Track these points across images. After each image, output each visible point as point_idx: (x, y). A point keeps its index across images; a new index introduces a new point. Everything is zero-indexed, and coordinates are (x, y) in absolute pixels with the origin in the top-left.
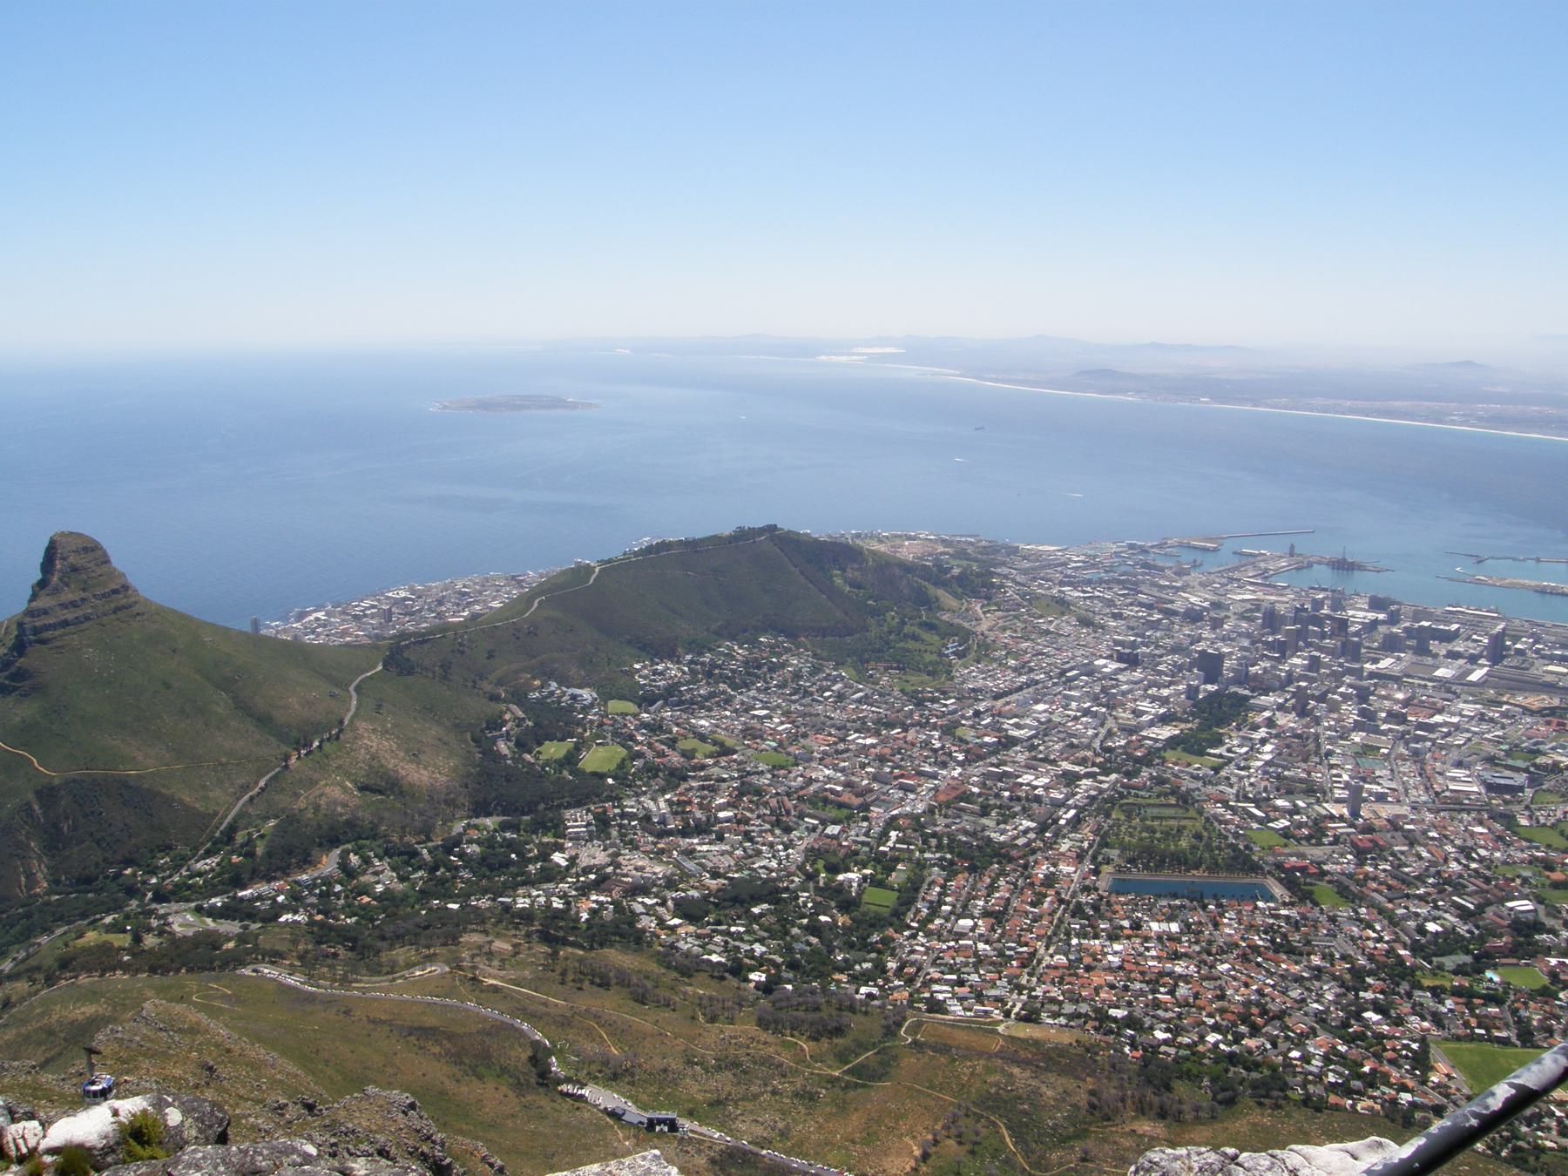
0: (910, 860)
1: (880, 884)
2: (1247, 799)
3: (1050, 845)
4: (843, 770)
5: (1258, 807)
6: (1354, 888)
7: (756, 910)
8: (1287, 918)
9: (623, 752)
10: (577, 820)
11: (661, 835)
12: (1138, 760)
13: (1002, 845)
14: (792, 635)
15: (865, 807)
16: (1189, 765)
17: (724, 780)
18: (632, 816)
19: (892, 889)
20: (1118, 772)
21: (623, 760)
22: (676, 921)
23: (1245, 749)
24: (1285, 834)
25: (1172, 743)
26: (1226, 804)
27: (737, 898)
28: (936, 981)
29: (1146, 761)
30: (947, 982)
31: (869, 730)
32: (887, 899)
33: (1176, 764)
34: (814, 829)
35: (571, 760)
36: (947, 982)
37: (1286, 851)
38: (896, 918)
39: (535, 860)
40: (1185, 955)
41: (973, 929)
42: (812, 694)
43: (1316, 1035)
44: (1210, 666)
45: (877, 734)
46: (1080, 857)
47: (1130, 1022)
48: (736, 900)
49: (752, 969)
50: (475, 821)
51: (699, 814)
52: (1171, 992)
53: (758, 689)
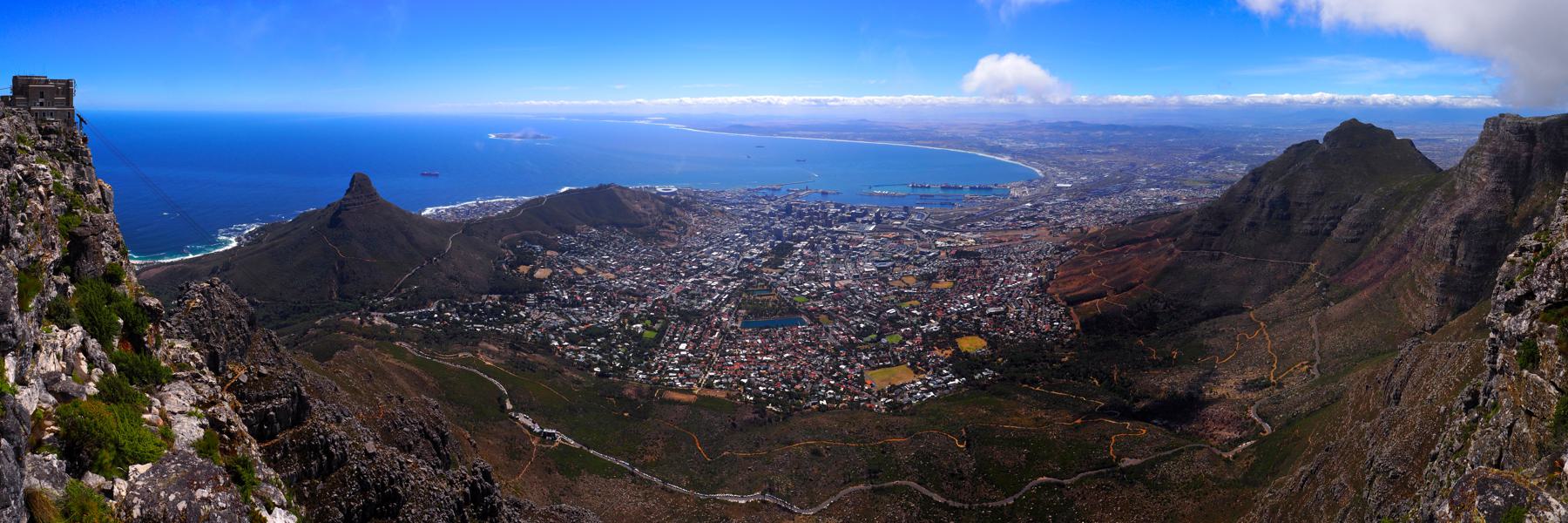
14: (619, 226)
24: (808, 297)
25: (765, 265)
27: (590, 334)
44: (778, 234)
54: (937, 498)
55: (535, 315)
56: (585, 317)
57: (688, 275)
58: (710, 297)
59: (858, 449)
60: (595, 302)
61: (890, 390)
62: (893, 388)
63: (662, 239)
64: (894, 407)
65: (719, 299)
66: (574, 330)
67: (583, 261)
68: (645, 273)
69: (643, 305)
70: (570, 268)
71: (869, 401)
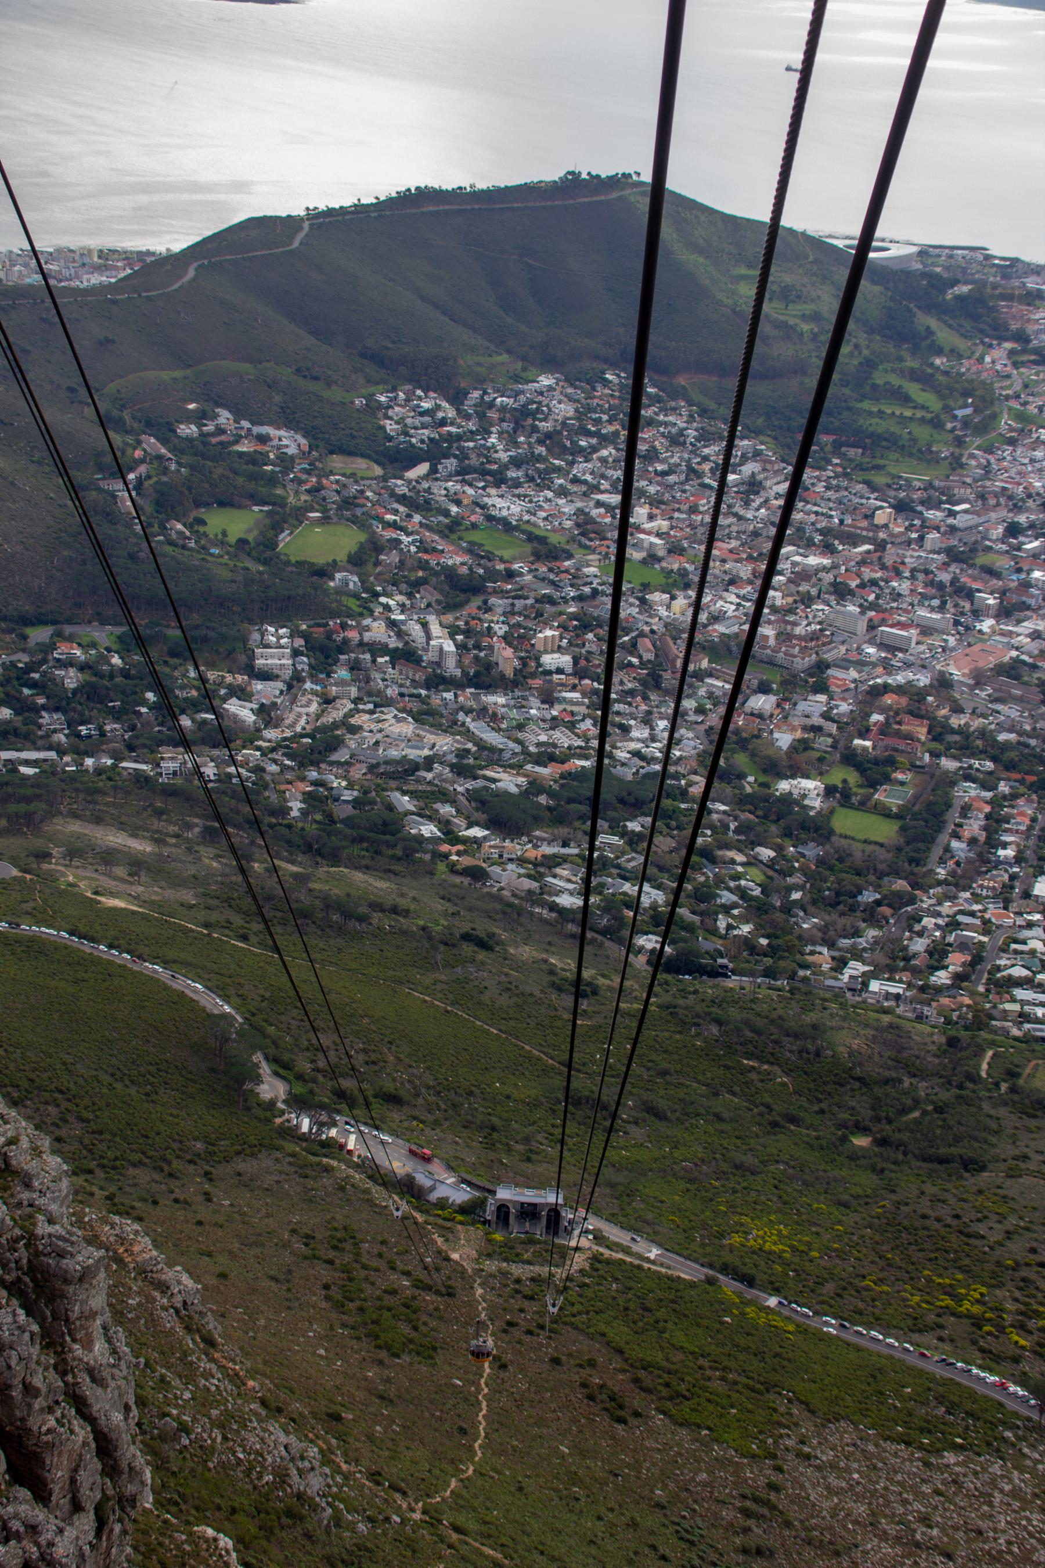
1: (863, 806)
7: (634, 826)
9: (363, 537)
10: (276, 647)
11: (437, 681)
17: (552, 601)
18: (376, 649)
19: (885, 813)
21: (362, 546)
22: (477, 832)
31: (810, 544)
32: (885, 831)
35: (264, 547)
39: (194, 706)
42: (699, 475)
45: (828, 549)
50: (68, 629)
51: (509, 652)
53: (603, 460)
55: (303, 715)
57: (1009, 611)
63: (877, 444)
67: (506, 506)
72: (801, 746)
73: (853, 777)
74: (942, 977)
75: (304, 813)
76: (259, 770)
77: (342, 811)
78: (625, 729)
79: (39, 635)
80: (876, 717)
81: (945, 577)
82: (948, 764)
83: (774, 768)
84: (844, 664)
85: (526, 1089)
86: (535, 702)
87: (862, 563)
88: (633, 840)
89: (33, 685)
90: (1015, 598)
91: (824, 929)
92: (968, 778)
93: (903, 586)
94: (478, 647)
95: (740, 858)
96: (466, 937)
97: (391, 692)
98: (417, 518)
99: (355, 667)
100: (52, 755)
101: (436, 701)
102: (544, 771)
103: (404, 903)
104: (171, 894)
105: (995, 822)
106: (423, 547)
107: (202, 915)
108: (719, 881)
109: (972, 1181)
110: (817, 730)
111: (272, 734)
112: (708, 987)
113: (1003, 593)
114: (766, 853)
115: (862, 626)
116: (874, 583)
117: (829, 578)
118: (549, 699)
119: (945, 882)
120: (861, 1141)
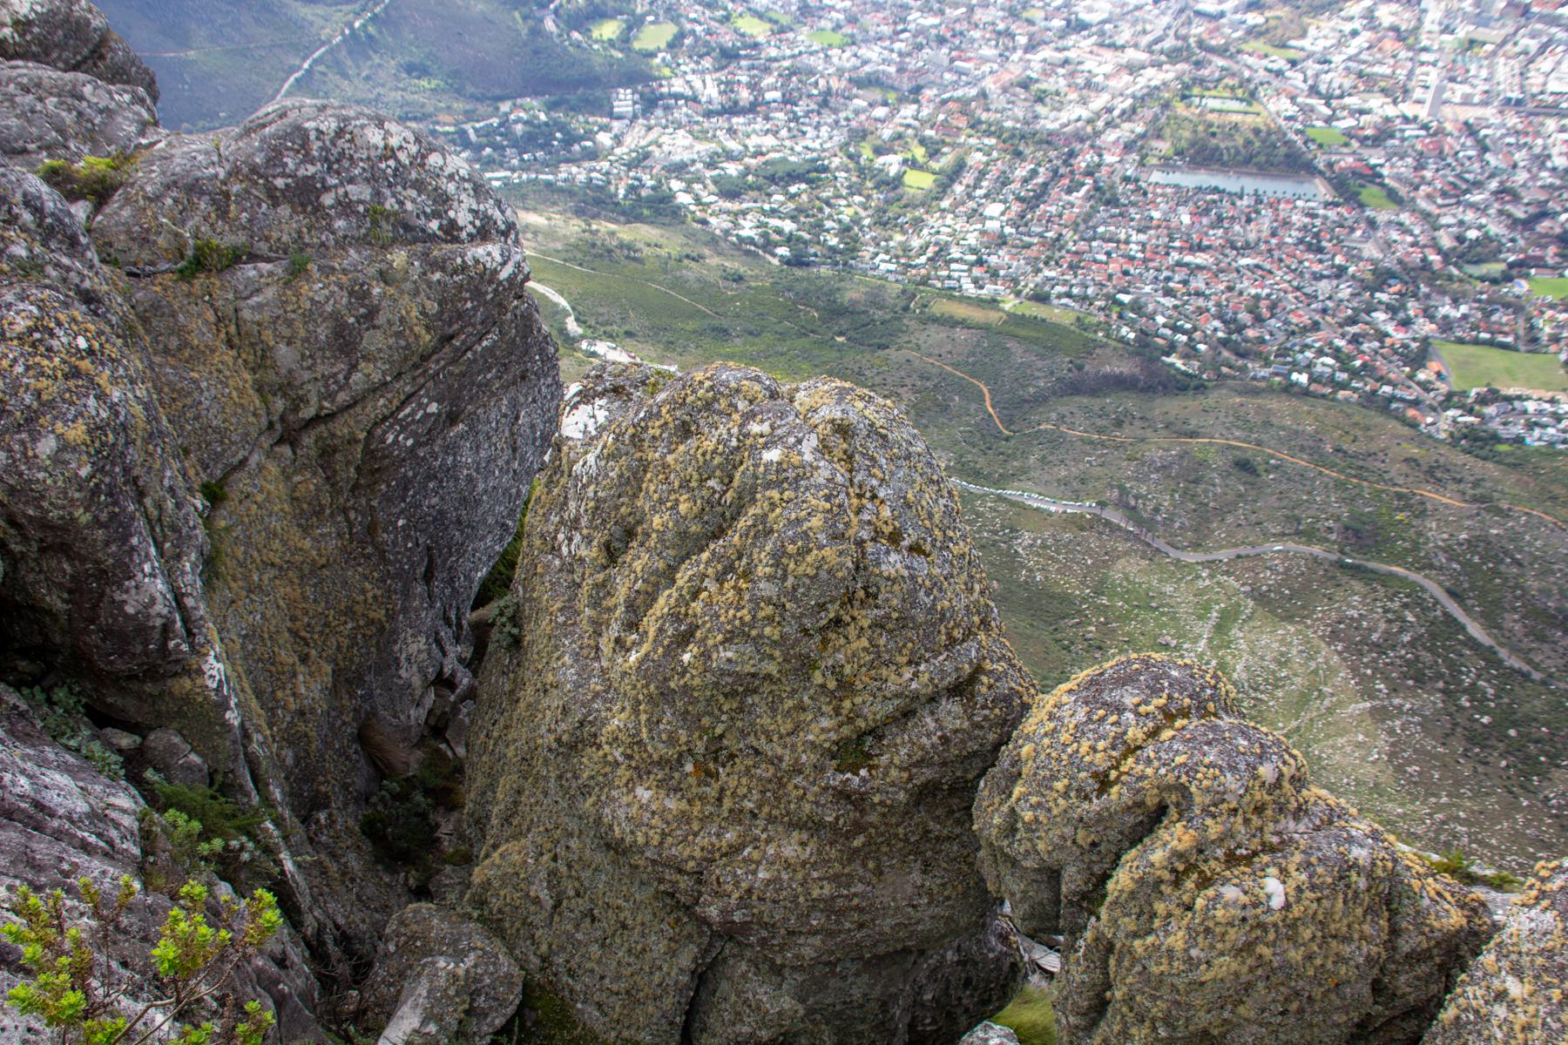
0: (953, 145)
2: (1318, 94)
3: (1097, 134)
4: (900, 54)
5: (1328, 104)
6: (1403, 191)
7: (793, 189)
8: (1326, 218)
10: (624, 100)
11: (708, 114)
12: (1211, 50)
13: (1050, 134)
15: (917, 90)
16: (1266, 56)
17: (776, 60)
18: (677, 97)
19: (934, 173)
20: (1186, 60)
22: (713, 198)
23: (1328, 43)
24: (1349, 134)
26: (1293, 99)
28: (956, 261)
29: (1222, 51)
30: (965, 262)
31: (931, 10)
33: (1250, 55)
34: (864, 111)
36: (965, 262)
37: (1345, 150)
38: (930, 201)
40: (1209, 247)
41: (1003, 214)
43: (1318, 330)
46: (1128, 147)
47: (1137, 307)
48: (772, 179)
49: (777, 245)
50: (519, 101)
52: (1185, 283)
54: (1475, 630)
55: (636, 138)
56: (761, 140)
57: (1031, 47)
58: (1084, 102)
59: (1339, 485)
60: (788, 101)
61: (1483, 400)
62: (1491, 397)
64: (1478, 441)
65: (1110, 110)
66: (732, 169)
68: (922, 31)
69: (908, 111)
70: (727, 18)
71: (1416, 403)
72: (900, 136)
73: (919, 153)
74: (923, 259)
75: (626, 197)
76: (608, 173)
77: (644, 193)
78: (804, 133)
79: (505, 107)
80: (941, 117)
81: (1001, 26)
82: (972, 141)
83: (879, 151)
84: (931, 84)
85: (691, 325)
86: (759, 119)
87: (957, 20)
88: (792, 197)
89: (501, 135)
90: (1038, 37)
91: (874, 239)
92: (978, 150)
93: (976, 34)
94: (732, 91)
95: (843, 202)
96: (688, 257)
97: (684, 120)
98: (708, 13)
99: (667, 108)
100: (508, 173)
101: (706, 125)
102: (753, 162)
103: (662, 241)
104: (551, 245)
105: (982, 174)
106: (709, 32)
107: (564, 255)
108: (830, 217)
109: (880, 353)
110: (908, 126)
111: (618, 151)
112: (799, 272)
113: (1031, 37)
114: (857, 199)
115: (946, 62)
116: (961, 33)
117: (934, 32)
118: (767, 119)
119: (943, 211)
120: (840, 339)
